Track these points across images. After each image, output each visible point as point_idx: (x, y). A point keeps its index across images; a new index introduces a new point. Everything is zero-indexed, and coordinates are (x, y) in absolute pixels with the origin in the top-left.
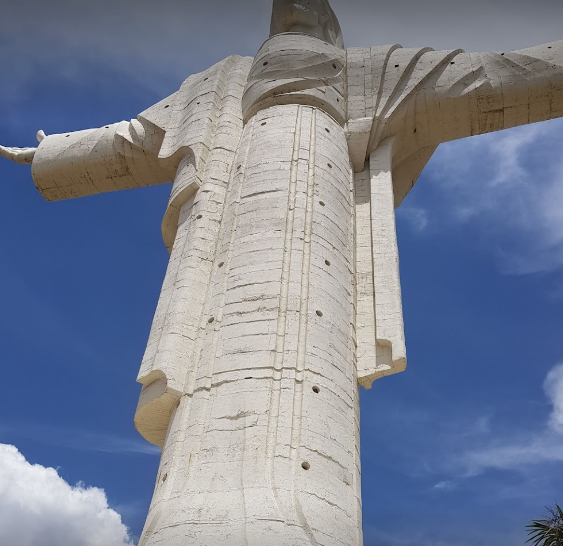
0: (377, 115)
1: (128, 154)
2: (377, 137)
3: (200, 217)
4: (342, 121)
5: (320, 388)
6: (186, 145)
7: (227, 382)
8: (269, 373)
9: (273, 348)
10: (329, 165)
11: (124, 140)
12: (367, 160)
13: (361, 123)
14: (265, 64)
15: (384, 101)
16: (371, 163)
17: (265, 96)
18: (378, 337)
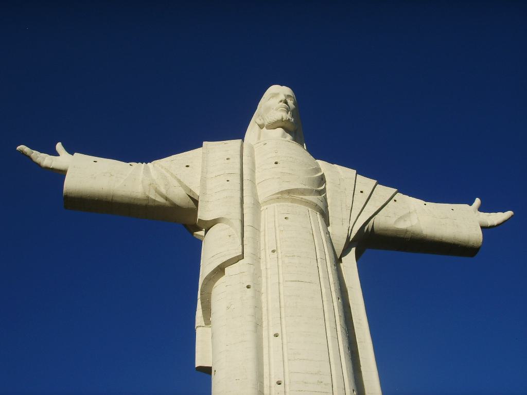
1: (153, 196)
3: (248, 287)
6: (227, 217)
17: (282, 193)
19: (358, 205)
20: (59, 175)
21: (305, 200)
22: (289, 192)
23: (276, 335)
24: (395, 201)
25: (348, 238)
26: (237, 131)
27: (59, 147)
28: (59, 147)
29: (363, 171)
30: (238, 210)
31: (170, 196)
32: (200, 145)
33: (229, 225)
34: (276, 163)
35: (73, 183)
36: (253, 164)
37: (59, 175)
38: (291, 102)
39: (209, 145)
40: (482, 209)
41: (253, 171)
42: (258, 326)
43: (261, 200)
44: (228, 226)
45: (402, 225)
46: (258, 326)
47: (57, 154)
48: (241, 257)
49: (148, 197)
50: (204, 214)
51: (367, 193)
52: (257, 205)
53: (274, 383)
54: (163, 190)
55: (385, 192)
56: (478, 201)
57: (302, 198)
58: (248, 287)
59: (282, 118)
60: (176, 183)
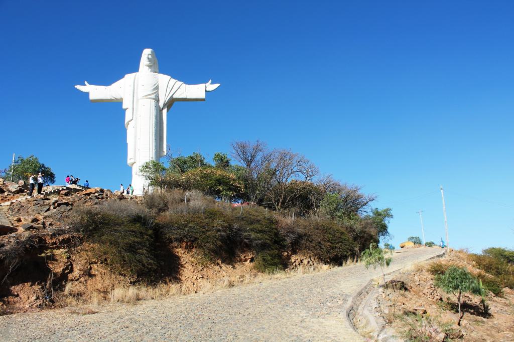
20: (87, 94)
25: (164, 103)
26: (135, 69)
27: (86, 83)
28: (86, 83)
29: (173, 77)
30: (132, 105)
31: (117, 98)
32: (123, 77)
35: (92, 97)
36: (138, 85)
37: (87, 94)
38: (150, 57)
39: (126, 76)
40: (211, 84)
41: (137, 89)
42: (136, 137)
43: (139, 98)
45: (181, 97)
46: (136, 137)
47: (85, 85)
48: (132, 120)
50: (124, 107)
52: (138, 100)
55: (179, 83)
56: (210, 80)
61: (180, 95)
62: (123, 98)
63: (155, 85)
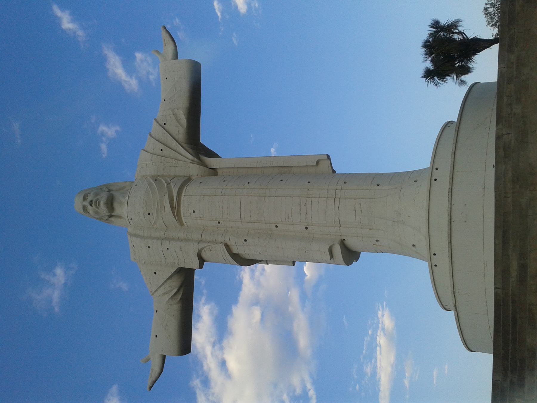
0: (190, 161)
1: (179, 296)
2: (203, 164)
3: (246, 240)
4: (188, 180)
5: (344, 181)
6: (197, 251)
7: (339, 217)
8: (337, 200)
9: (326, 199)
10: (224, 181)
11: (172, 298)
12: (211, 168)
13: (194, 170)
14: (149, 214)
15: (181, 158)
16: (214, 167)
17: (173, 213)
18: (315, 165)
19: (173, 154)
21: (177, 196)
22: (172, 208)
23: (277, 226)
24: (165, 124)
33: (202, 250)
34: (149, 214)
44: (203, 251)
45: (184, 121)
49: (181, 299)
51: (162, 147)
53: (307, 231)
54: (175, 290)
57: (176, 199)
58: (246, 240)
59: (106, 204)
60: (169, 281)
61: (179, 121)
62: (175, 269)
63: (150, 185)
